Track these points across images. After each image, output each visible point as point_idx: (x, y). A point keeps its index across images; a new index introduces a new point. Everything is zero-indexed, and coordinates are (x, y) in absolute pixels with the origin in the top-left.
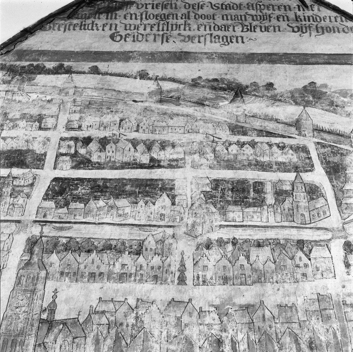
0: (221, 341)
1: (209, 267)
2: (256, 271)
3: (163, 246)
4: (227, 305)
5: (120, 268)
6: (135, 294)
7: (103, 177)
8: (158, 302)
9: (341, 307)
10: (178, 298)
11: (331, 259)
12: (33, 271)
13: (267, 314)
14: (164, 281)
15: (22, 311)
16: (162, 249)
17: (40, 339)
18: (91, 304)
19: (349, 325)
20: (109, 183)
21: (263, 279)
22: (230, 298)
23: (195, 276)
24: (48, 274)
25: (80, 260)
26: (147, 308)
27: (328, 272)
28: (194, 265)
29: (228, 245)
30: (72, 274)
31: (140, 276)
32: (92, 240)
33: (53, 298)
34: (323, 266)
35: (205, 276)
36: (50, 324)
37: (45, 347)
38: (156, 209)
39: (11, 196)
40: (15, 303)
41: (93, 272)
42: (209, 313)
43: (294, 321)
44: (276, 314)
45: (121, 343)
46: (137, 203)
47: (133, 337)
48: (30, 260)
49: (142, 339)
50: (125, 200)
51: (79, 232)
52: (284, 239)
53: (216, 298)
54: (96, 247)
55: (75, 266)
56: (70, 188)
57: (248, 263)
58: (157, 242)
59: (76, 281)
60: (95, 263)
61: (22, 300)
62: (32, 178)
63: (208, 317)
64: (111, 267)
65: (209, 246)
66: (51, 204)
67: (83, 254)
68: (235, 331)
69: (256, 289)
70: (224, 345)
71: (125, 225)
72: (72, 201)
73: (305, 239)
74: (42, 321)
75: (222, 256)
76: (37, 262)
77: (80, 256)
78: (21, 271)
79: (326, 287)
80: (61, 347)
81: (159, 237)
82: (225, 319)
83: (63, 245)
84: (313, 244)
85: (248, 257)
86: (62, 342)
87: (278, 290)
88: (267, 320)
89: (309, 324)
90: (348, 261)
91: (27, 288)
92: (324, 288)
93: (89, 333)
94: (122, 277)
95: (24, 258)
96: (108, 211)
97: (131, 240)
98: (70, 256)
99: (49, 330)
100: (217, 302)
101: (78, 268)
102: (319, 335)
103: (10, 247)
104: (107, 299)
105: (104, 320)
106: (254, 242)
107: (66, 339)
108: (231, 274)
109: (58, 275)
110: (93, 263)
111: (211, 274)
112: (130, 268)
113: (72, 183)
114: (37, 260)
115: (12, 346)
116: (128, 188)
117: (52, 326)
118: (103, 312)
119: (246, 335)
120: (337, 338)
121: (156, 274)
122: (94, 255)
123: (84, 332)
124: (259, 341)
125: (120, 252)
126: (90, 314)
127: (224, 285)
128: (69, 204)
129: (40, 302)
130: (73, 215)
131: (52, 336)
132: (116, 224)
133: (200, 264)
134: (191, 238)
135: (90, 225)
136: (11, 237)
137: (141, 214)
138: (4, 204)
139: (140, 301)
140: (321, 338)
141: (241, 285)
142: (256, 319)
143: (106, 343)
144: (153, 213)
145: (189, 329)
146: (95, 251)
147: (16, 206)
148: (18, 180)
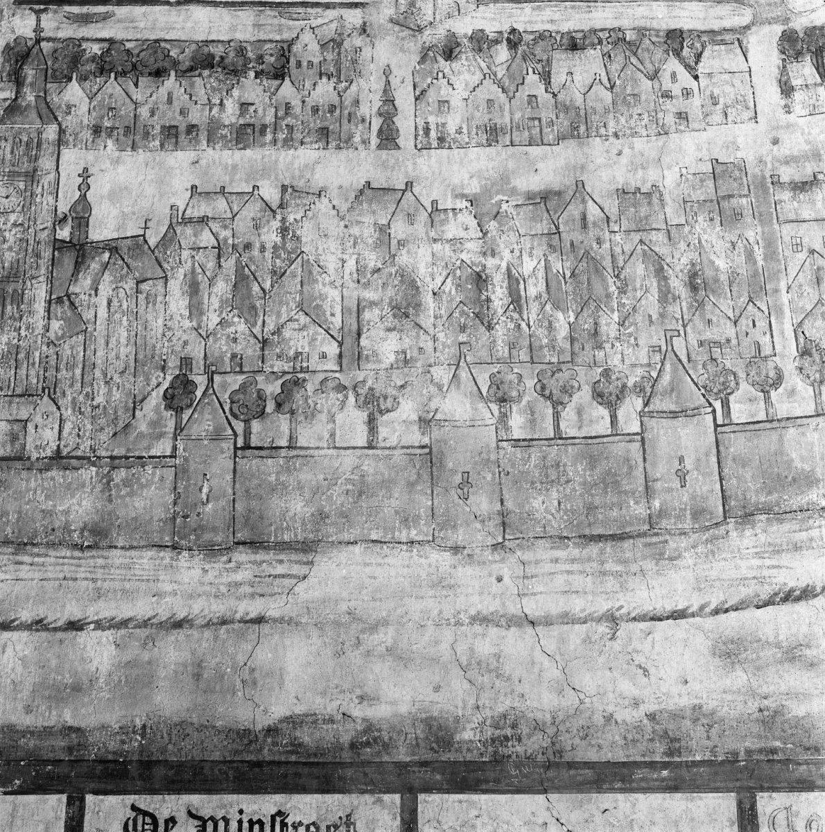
0: (484, 277)
1: (452, 103)
2: (567, 109)
3: (339, 54)
4: (498, 193)
5: (238, 113)
6: (277, 175)
8: (334, 193)
9: (766, 191)
10: (380, 181)
11: (748, 74)
12: (27, 126)
13: (593, 212)
14: (346, 142)
15: (9, 225)
16: (338, 63)
17: (61, 285)
18: (172, 201)
19: (784, 232)
21: (582, 128)
22: (505, 178)
23: (420, 128)
24: (64, 132)
25: (138, 95)
26: (308, 208)
27: (739, 107)
28: (416, 99)
29: (499, 47)
30: (121, 131)
31: (286, 131)
32: (163, 44)
33: (79, 190)
34: (727, 93)
35: (444, 125)
37: (72, 304)
41: (173, 123)
42: (455, 215)
43: (653, 226)
44: (613, 210)
45: (249, 289)
47: (278, 275)
49: (299, 279)
52: (634, 29)
53: (471, 177)
54: (175, 63)
55: (126, 110)
57: (546, 91)
58: (323, 46)
59: (134, 148)
60: (175, 103)
61: (7, 197)
63: (452, 222)
64: (215, 110)
65: (451, 51)
67: (143, 81)
68: (517, 253)
69: (566, 153)
70: (490, 287)
73: (686, 27)
75: (485, 75)
76: (33, 103)
77: (136, 85)
79: (734, 143)
81: (329, 31)
82: (492, 226)
83: (93, 59)
84: (704, 38)
85: (546, 77)
86: (111, 293)
87: (619, 154)
88: (590, 225)
89: (690, 232)
90: (789, 78)
91: (17, 169)
92: (728, 147)
94: (245, 135)
98: (112, 87)
99: (78, 265)
100: (474, 187)
101: (135, 115)
102: (713, 257)
104: (210, 188)
105: (206, 239)
106: (562, 37)
107: (120, 285)
108: (507, 120)
109: (87, 135)
110: (170, 101)
111: (458, 121)
112: (260, 111)
114: (33, 99)
117: (84, 256)
118: (203, 220)
119: (543, 263)
120: (755, 263)
121: (326, 124)
122: (171, 82)
123: (161, 267)
124: (573, 275)
125: (236, 72)
126: (171, 224)
127: (490, 145)
129: (51, 200)
131: (85, 278)
133: (432, 96)
134: (407, 32)
140: (717, 262)
141: (530, 145)
142: (566, 223)
143: (215, 290)
145: (408, 252)
146: (173, 73)
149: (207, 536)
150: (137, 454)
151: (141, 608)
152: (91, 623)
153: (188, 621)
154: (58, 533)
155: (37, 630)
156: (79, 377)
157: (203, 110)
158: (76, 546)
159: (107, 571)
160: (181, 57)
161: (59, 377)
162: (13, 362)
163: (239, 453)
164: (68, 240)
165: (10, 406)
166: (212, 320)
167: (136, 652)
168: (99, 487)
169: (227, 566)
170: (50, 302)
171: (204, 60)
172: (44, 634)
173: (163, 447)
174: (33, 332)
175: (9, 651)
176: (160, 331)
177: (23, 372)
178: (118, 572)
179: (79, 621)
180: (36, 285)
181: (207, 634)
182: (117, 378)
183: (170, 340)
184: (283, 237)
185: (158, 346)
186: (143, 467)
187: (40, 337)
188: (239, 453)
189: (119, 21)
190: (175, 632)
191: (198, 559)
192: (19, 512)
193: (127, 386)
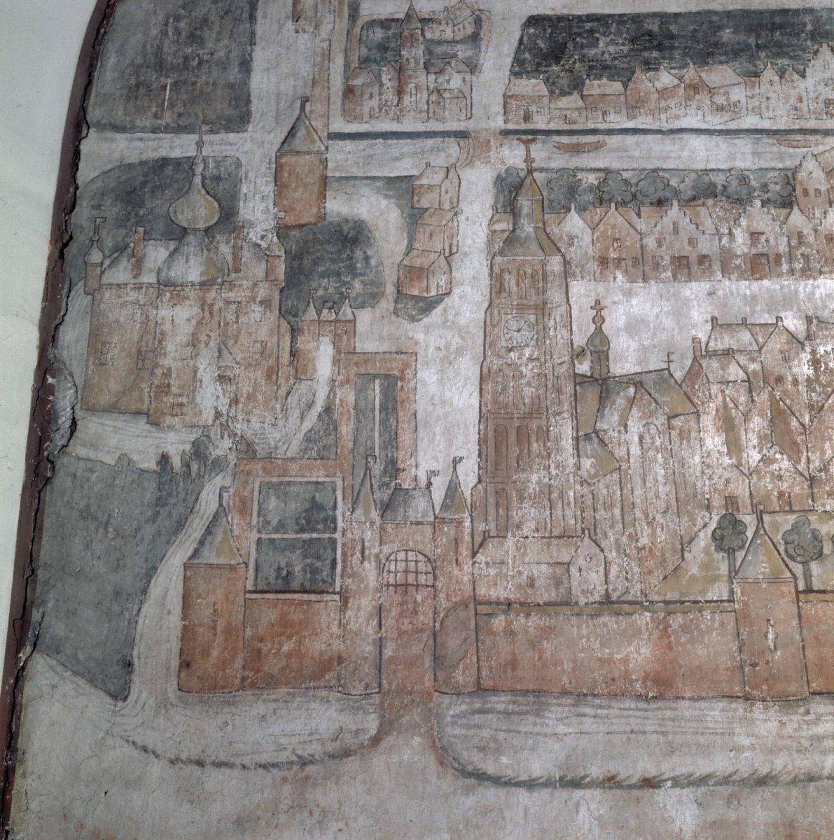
5: (749, 242)
7: (657, 9)
15: (524, 359)
18: (694, 332)
20: (676, 23)
24: (569, 263)
25: (641, 225)
30: (629, 262)
31: (802, 261)
32: (661, 174)
33: (594, 322)
36: (601, 386)
37: (601, 441)
38: (811, 89)
39: (426, 68)
40: (503, 339)
41: (683, 254)
46: (757, 74)
48: (514, 230)
50: (725, 67)
51: (628, 155)
54: (677, 193)
55: (631, 241)
56: (575, 44)
59: (645, 279)
60: (682, 233)
62: (470, 19)
64: (725, 240)
66: (532, 86)
67: (645, 211)
71: (738, 132)
72: (588, 76)
74: (580, 380)
76: (533, 235)
77: (639, 215)
78: (498, 259)
80: (641, 439)
83: (591, 189)
86: (641, 429)
91: (525, 302)
93: (703, 403)
94: (759, 265)
95: (498, 227)
96: (689, 98)
97: (761, 169)
98: (615, 218)
101: (642, 246)
103: (455, 200)
104: (732, 320)
105: (734, 372)
107: (650, 421)
109: (593, 266)
110: (676, 231)
113: (579, 27)
114: (532, 230)
115: (519, 442)
116: (727, 35)
117: (608, 391)
118: (728, 353)
122: (674, 212)
123: (691, 402)
125: (740, 201)
128: (583, 84)
129: (565, 332)
130: (600, 113)
131: (612, 414)
132: (715, 131)
135: (650, 137)
136: (452, 174)
137: (771, 101)
138: (414, 92)
139: (815, 321)
143: (751, 426)
144: (804, 99)
146: (675, 203)
147: (447, 95)
148: (434, 26)
149: (780, 687)
150: (692, 598)
151: (720, 764)
152: (668, 779)
153: (772, 778)
154: (620, 684)
155: (611, 788)
156: (619, 518)
157: (712, 240)
158: (639, 697)
159: (677, 724)
160: (682, 187)
161: (598, 517)
162: (546, 502)
163: (802, 596)
164: (589, 374)
165: (548, 547)
166: (754, 457)
167: (721, 812)
168: (656, 635)
169: (806, 718)
170: (577, 439)
171: (705, 190)
172: (619, 792)
173: (718, 591)
174: (564, 470)
175: (583, 811)
176: (699, 469)
177: (558, 512)
178: (689, 724)
179: (654, 778)
180: (561, 422)
181: (795, 792)
182: (659, 517)
183: (710, 478)
184: (816, 370)
185: (699, 484)
186: (700, 612)
187: (571, 475)
188: (802, 596)
189: (612, 150)
190: (760, 789)
191: (773, 712)
192: (574, 661)
193: (672, 526)
